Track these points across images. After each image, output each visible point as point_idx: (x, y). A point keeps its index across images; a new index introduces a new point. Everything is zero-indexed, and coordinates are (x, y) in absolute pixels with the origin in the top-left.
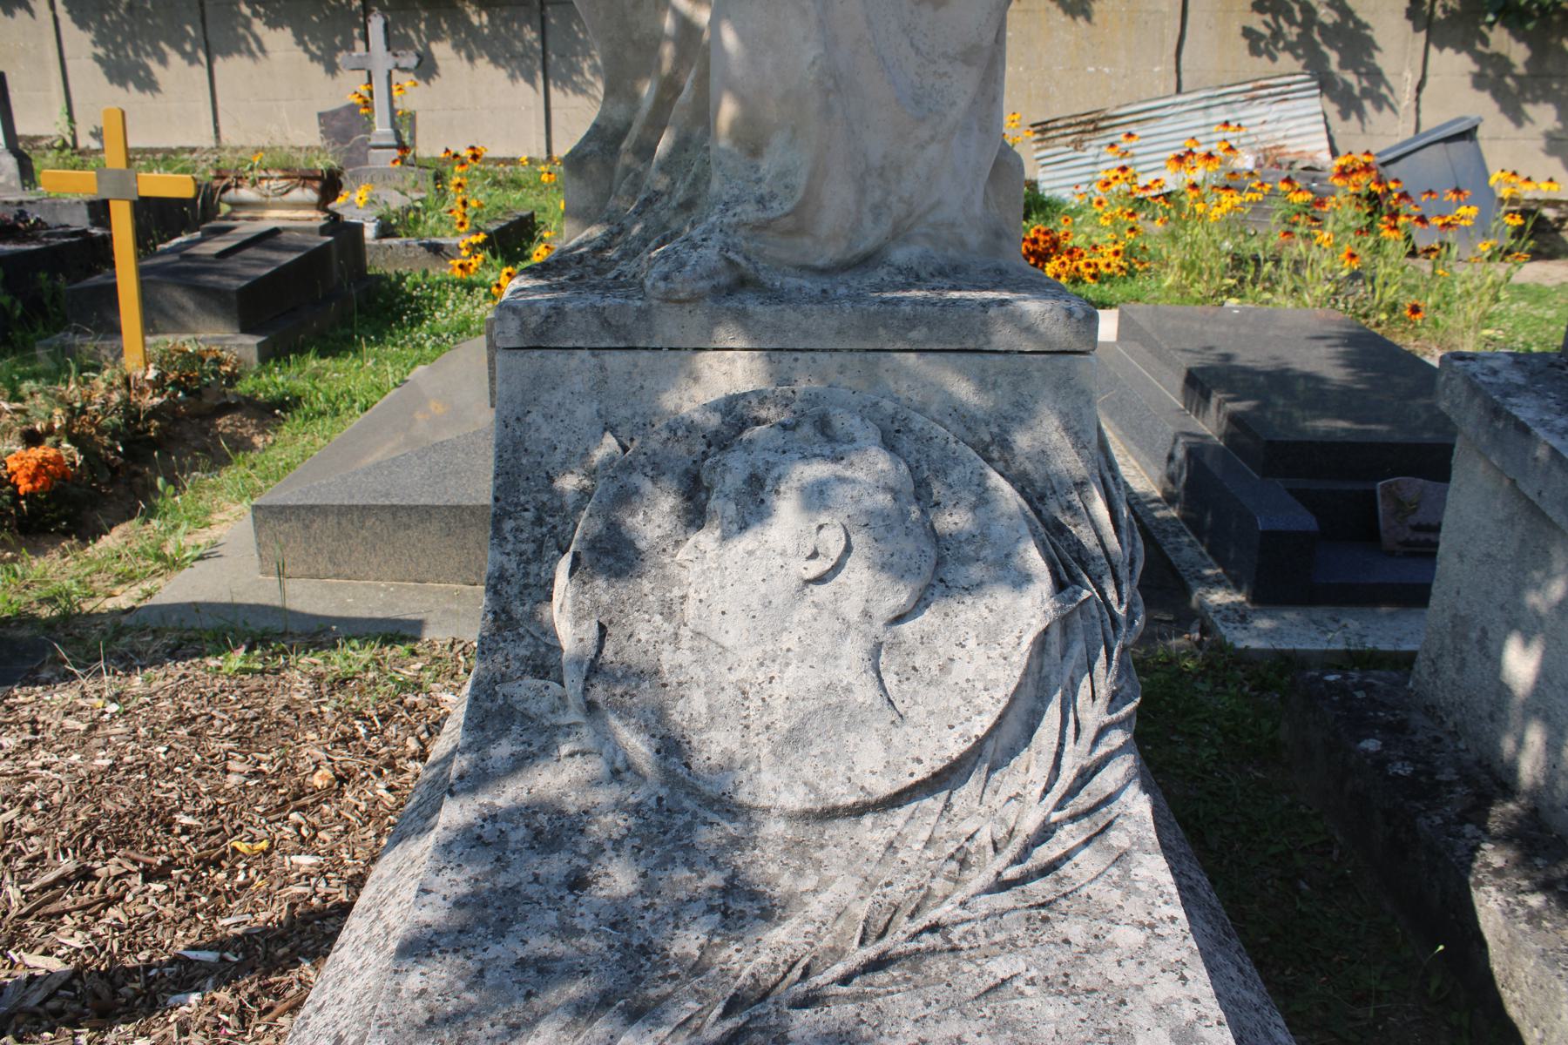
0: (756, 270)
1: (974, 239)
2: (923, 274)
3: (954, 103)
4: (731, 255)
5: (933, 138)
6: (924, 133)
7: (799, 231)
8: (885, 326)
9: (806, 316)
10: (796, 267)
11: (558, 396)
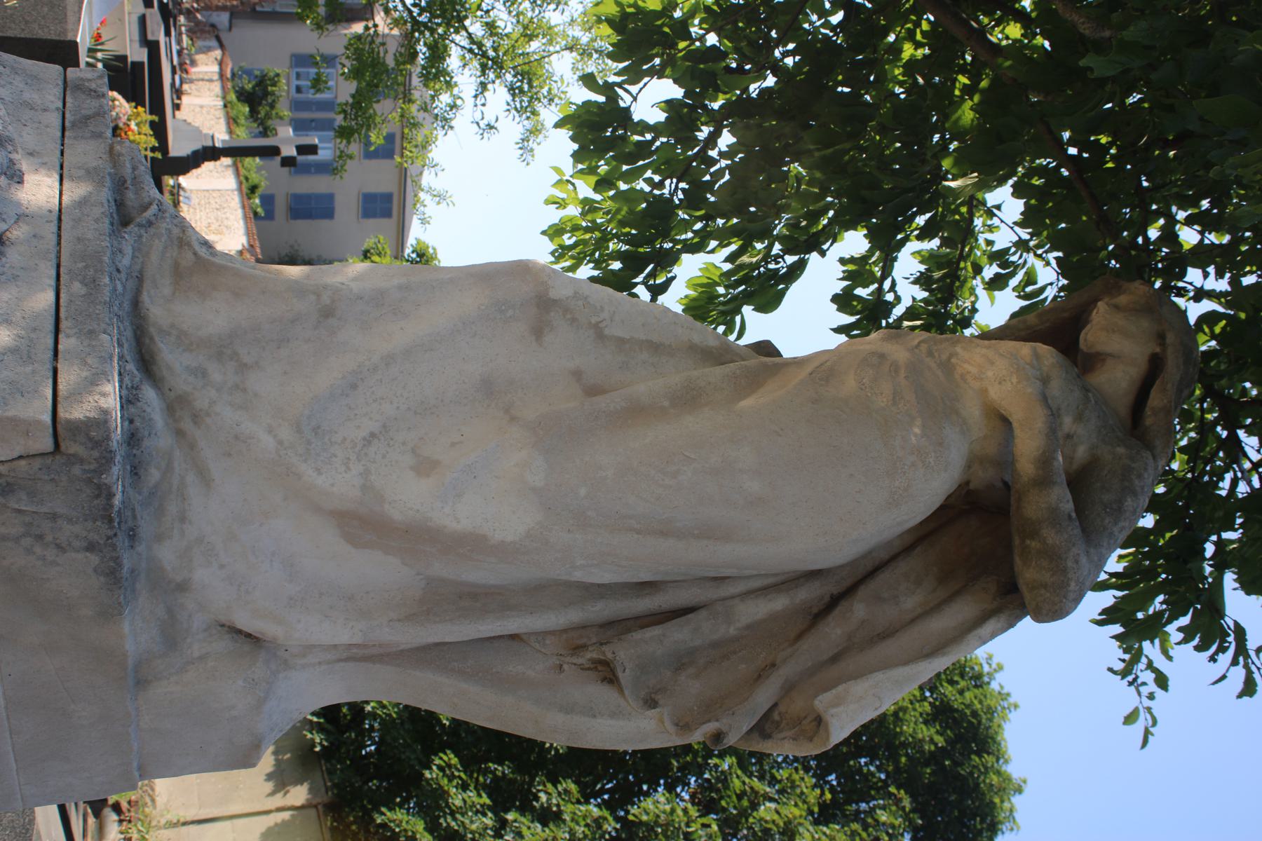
0: (140, 226)
1: (167, 554)
2: (132, 410)
3: (320, 473)
4: (154, 208)
5: (280, 443)
6: (286, 433)
7: (178, 273)
8: (86, 267)
9: (97, 221)
10: (141, 272)
11: (21, 86)
